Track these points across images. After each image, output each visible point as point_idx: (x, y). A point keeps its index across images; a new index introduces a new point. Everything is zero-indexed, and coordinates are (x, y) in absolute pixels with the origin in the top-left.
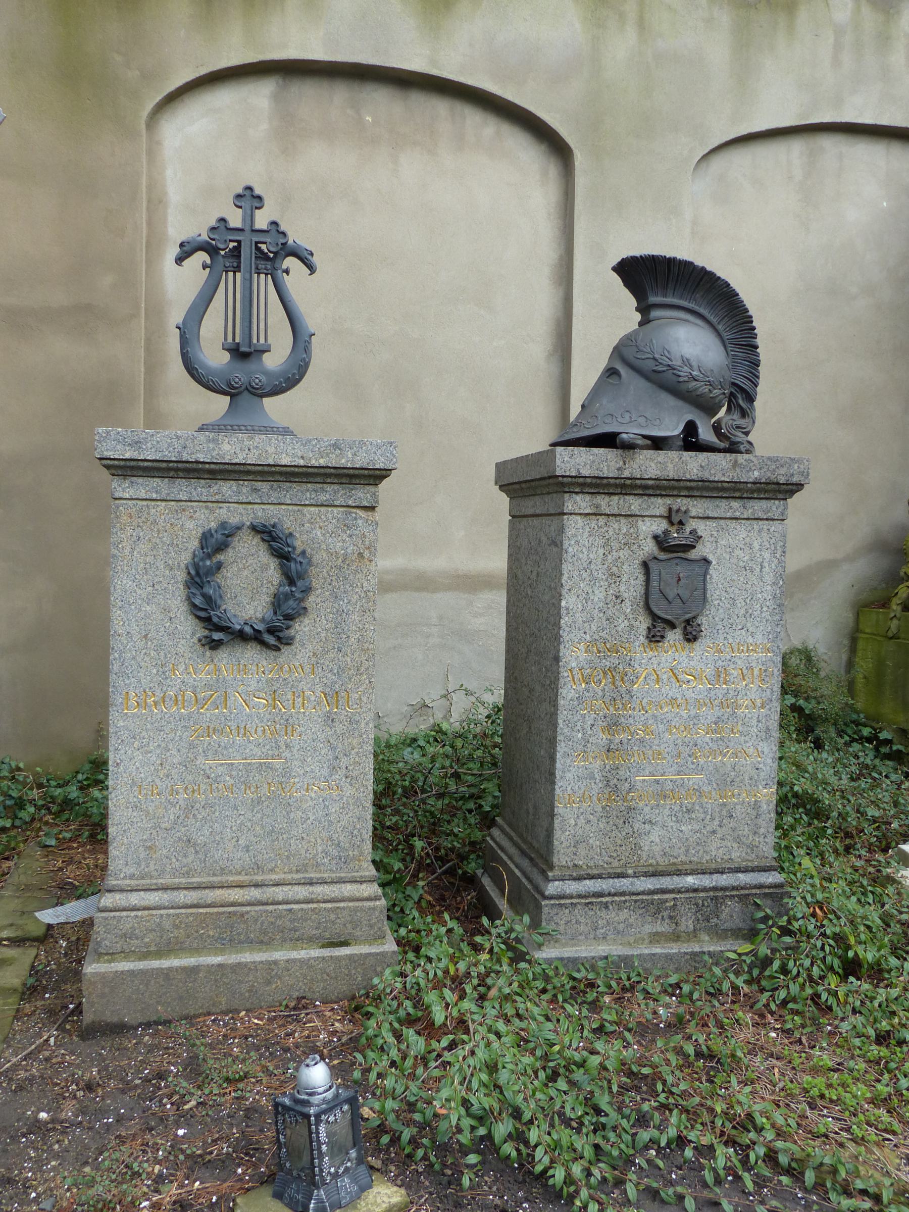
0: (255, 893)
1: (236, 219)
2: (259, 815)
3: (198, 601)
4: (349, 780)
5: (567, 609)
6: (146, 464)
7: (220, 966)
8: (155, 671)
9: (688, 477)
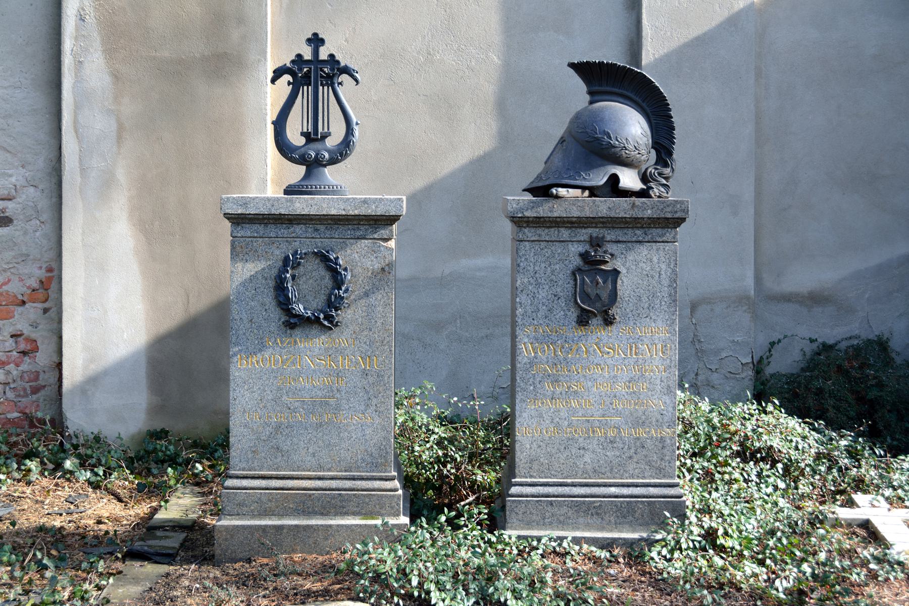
0: (319, 484)
1: (308, 55)
3: (281, 299)
5: (520, 303)
7: (296, 526)
9: (600, 215)
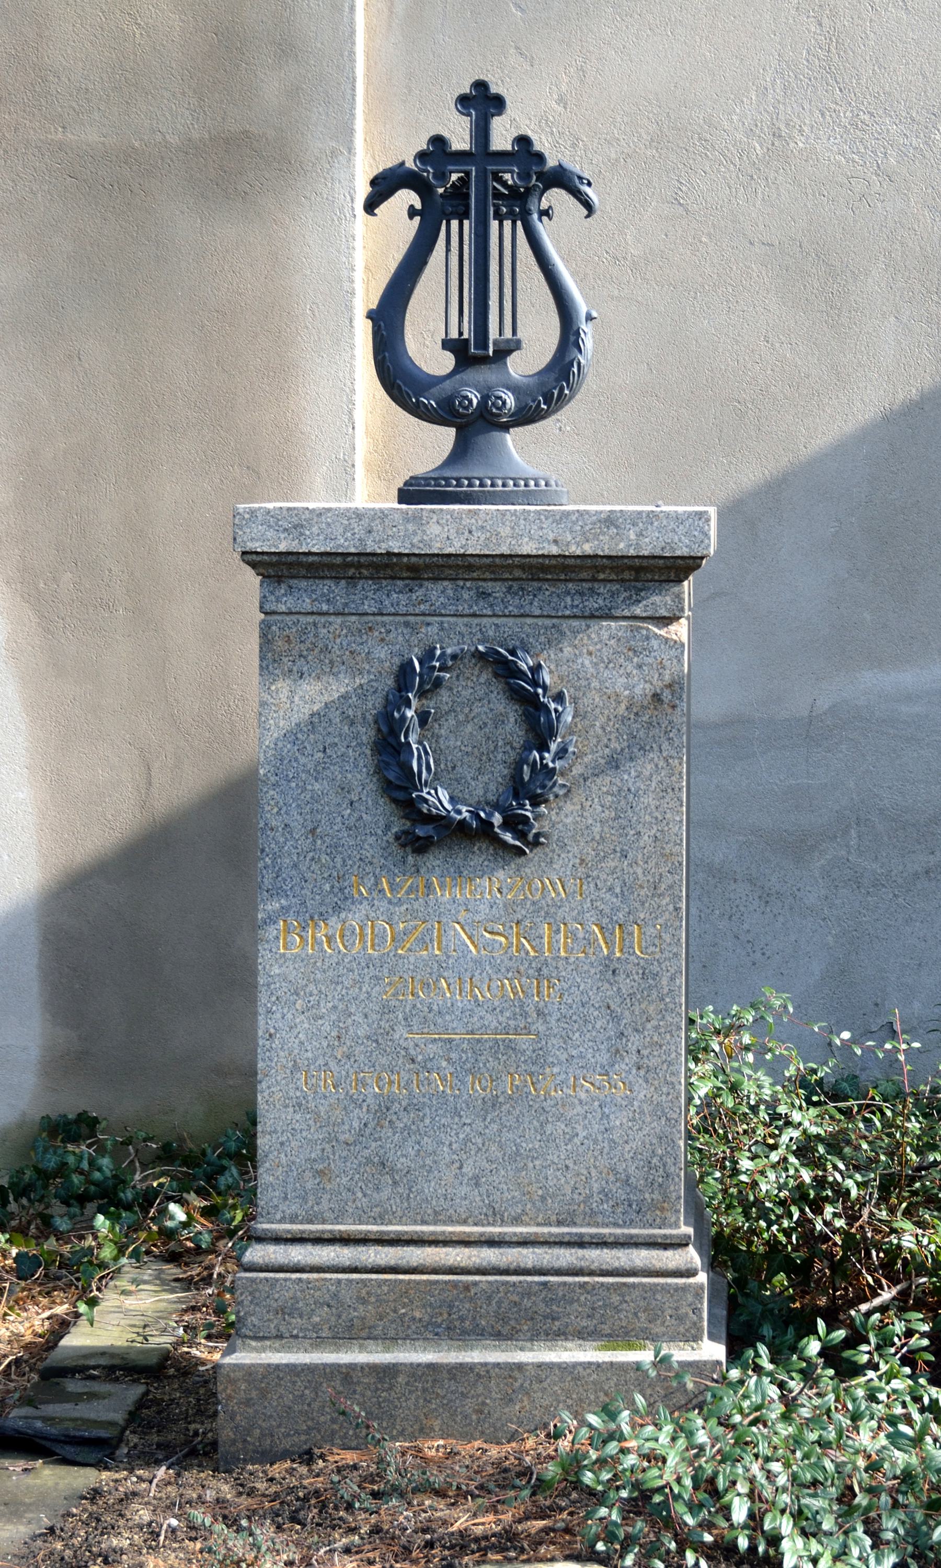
0: (489, 1256)
1: (460, 138)
2: (495, 1127)
3: (391, 776)
4: (642, 1072)
6: (311, 559)
7: (431, 1366)
8: (327, 887)
